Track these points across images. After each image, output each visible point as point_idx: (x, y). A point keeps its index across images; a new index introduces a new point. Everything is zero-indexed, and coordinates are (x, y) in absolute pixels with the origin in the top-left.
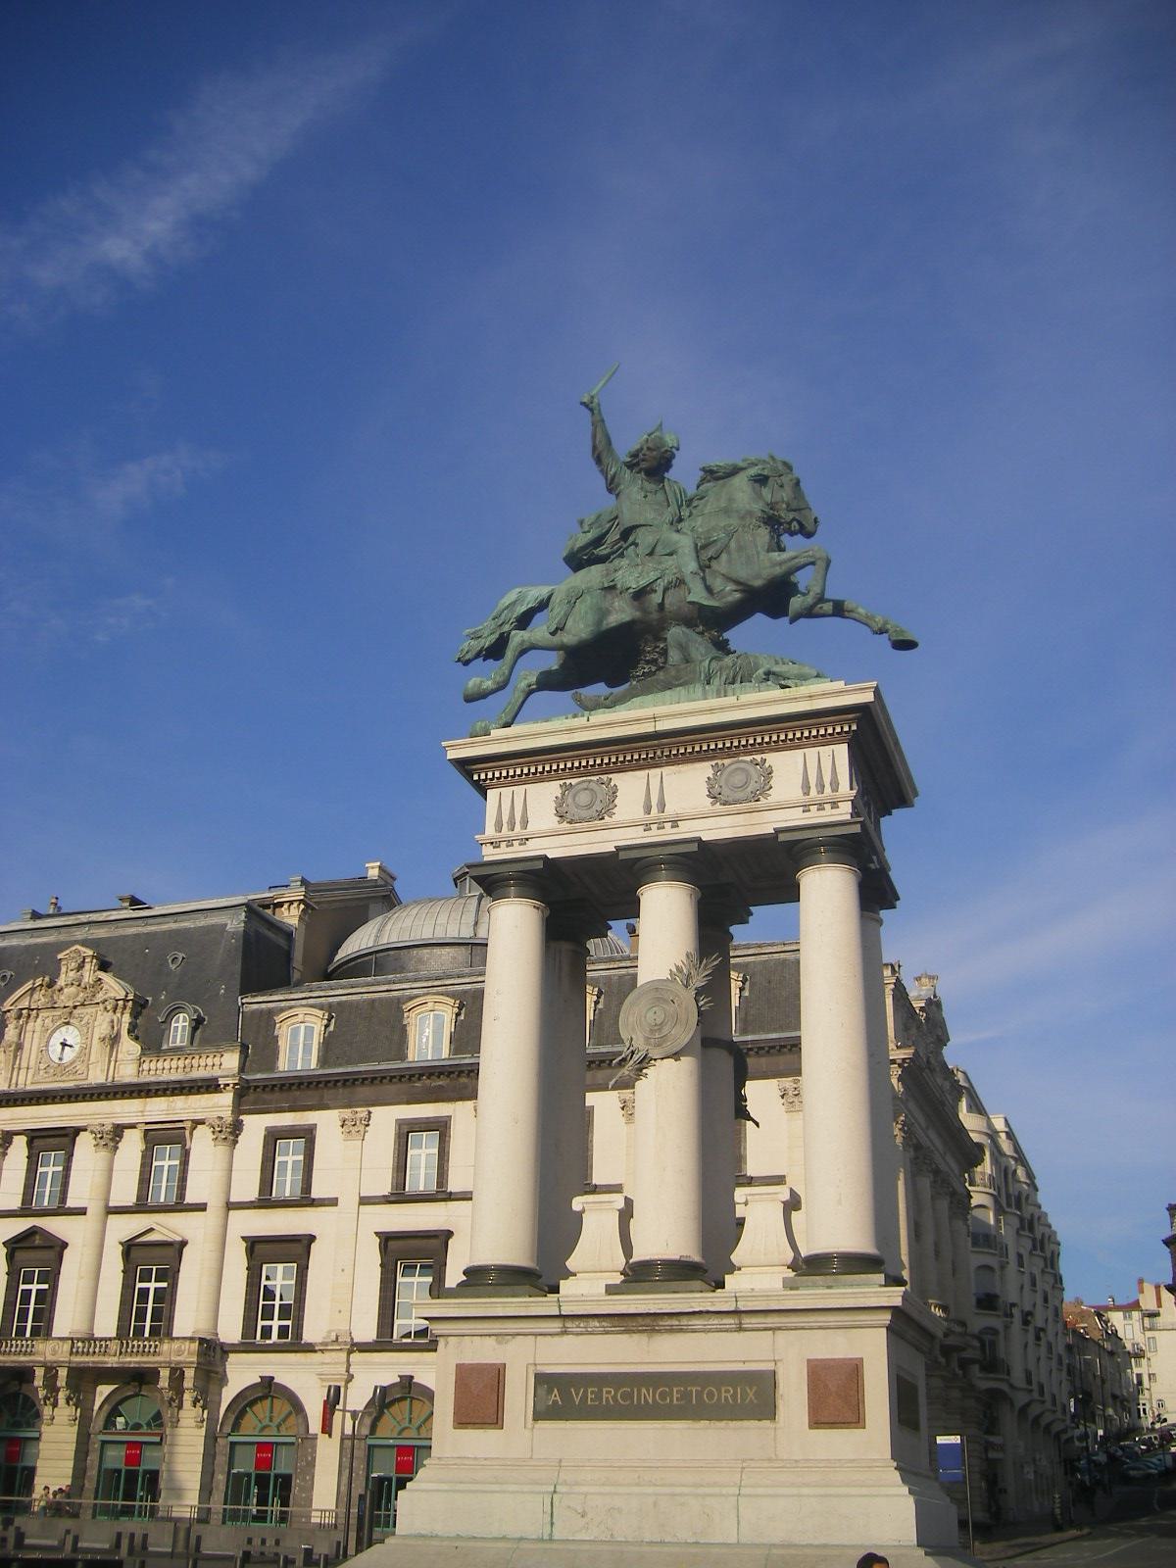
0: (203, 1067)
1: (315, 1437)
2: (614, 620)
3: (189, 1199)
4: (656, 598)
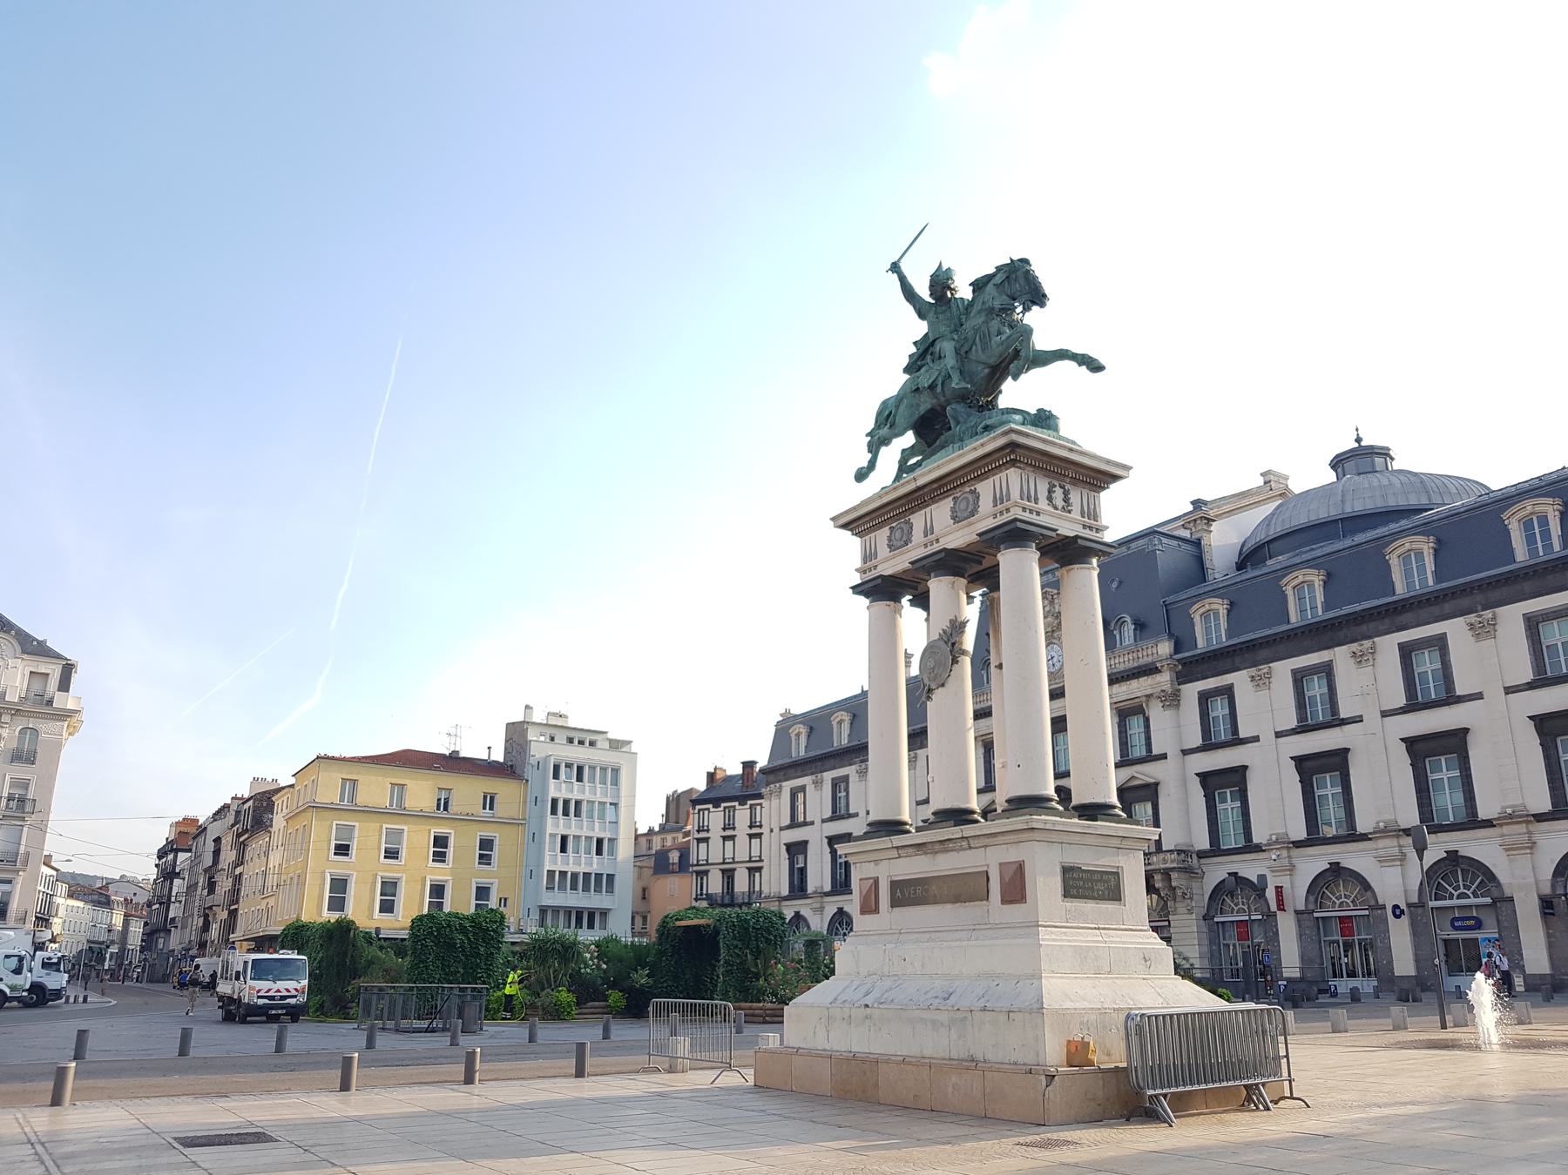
0: (1144, 659)
1: (1275, 915)
2: (923, 409)
3: (1155, 752)
4: (939, 389)
